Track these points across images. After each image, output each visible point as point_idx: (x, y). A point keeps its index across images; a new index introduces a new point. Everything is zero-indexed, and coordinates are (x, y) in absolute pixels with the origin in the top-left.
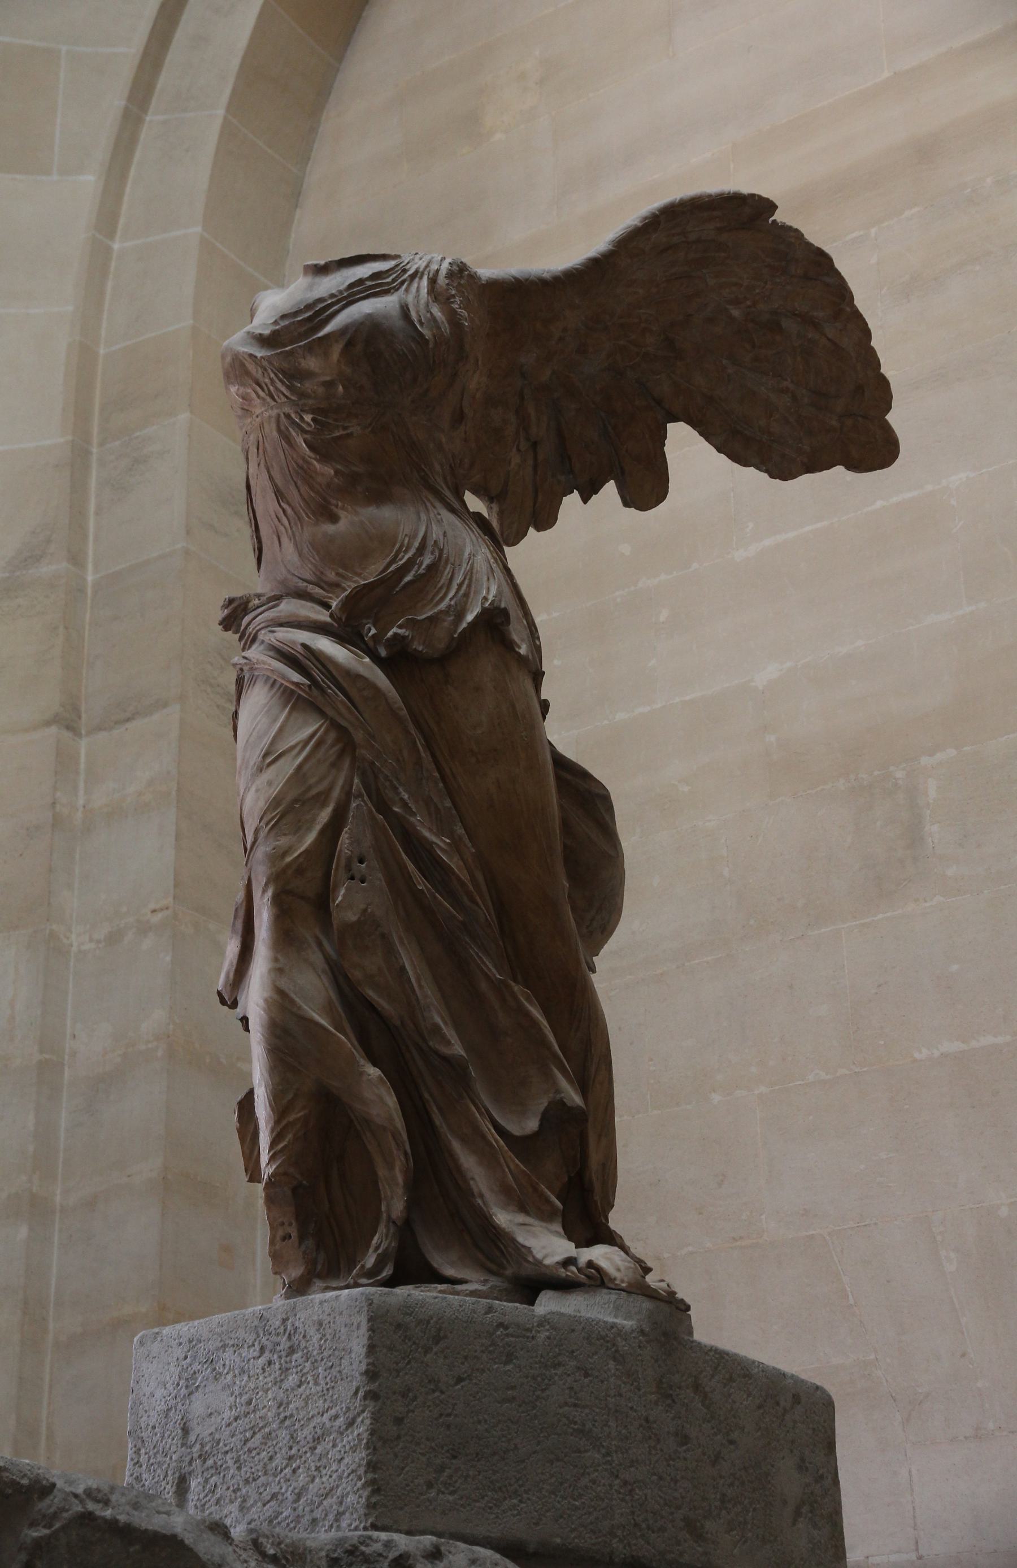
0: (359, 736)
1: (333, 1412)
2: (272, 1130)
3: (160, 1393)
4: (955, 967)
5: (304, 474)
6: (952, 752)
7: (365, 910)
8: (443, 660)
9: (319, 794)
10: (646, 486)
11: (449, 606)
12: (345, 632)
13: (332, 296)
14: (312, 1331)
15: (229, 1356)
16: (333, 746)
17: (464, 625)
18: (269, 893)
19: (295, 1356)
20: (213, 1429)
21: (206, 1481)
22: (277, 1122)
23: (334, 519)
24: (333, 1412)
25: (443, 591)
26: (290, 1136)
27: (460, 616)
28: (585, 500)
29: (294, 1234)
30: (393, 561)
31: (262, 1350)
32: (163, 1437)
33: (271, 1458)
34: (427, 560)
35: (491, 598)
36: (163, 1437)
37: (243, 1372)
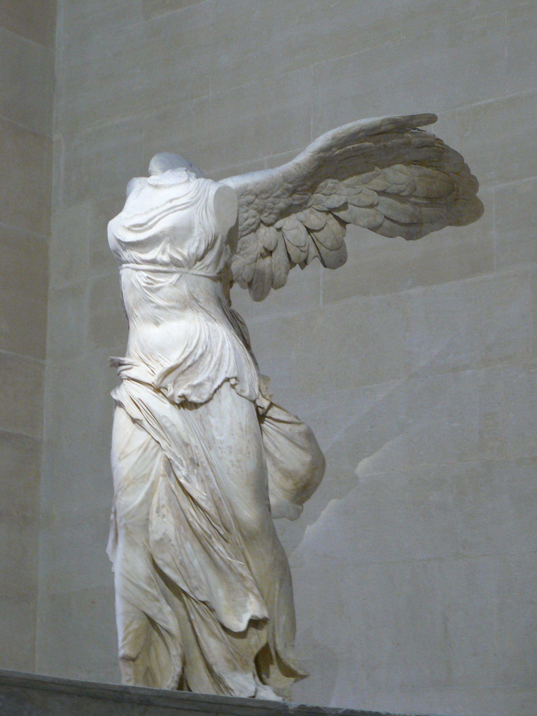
0: (164, 444)
7: (164, 534)
8: (207, 402)
9: (144, 476)
10: (335, 258)
11: (208, 378)
12: (158, 390)
13: (157, 208)
16: (152, 449)
17: (216, 386)
22: (124, 631)
25: (207, 368)
26: (130, 637)
27: (213, 382)
28: (302, 267)
30: (183, 353)
34: (199, 351)
35: (229, 371)
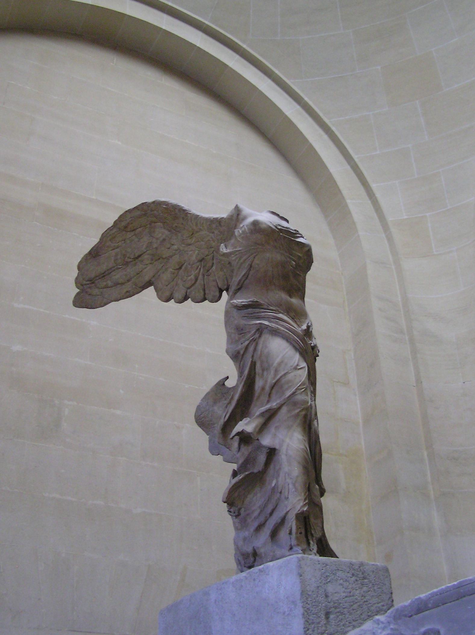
1: (382, 603)
2: (305, 495)
3: (313, 579)
4: (63, 471)
5: (285, 277)
6: (75, 403)
14: (371, 573)
15: (340, 573)
18: (303, 413)
19: (366, 581)
20: (337, 599)
21: (338, 616)
23: (291, 296)
24: (382, 603)
29: (303, 532)
31: (353, 575)
32: (317, 596)
33: (361, 614)
36: (317, 596)
37: (346, 581)
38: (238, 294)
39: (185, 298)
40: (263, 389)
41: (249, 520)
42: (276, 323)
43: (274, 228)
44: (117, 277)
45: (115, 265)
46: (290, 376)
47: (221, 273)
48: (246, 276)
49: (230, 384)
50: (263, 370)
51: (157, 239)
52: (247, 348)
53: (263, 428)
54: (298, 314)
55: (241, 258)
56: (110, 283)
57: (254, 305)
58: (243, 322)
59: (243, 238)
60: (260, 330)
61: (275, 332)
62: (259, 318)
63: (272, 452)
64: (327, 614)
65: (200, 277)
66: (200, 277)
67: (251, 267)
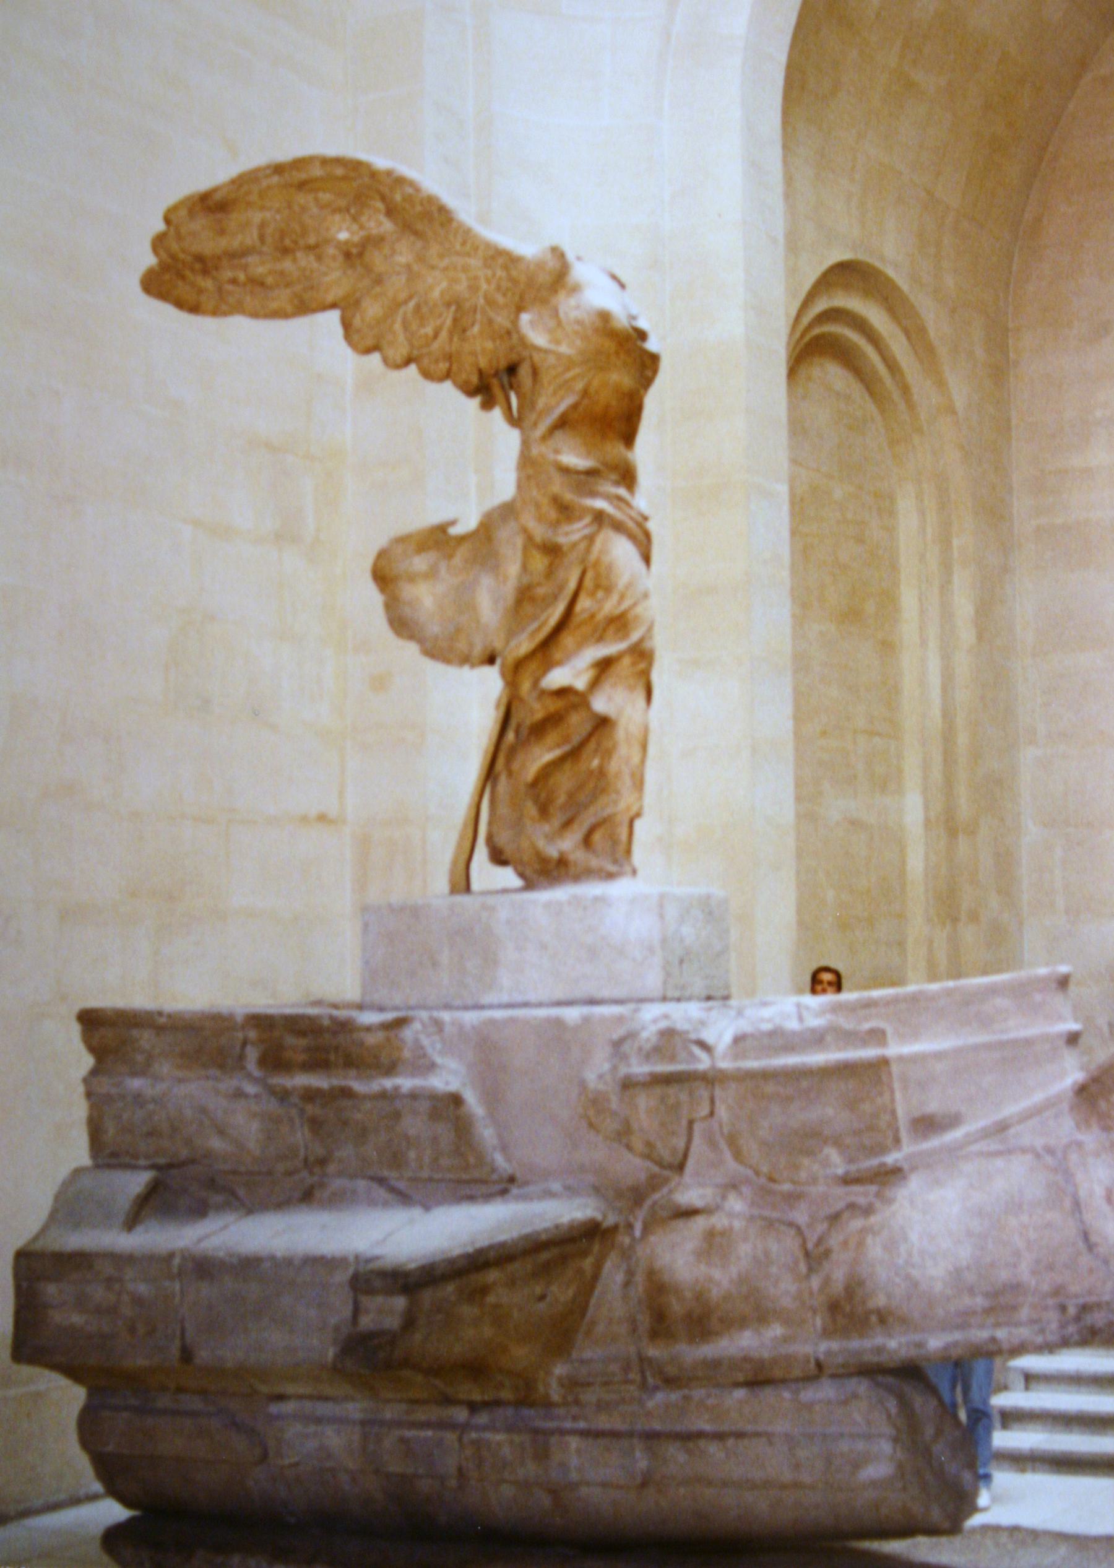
38: (559, 435)
39: (407, 362)
40: (592, 616)
41: (551, 810)
42: (619, 508)
43: (631, 331)
44: (261, 270)
45: (258, 243)
46: (639, 610)
47: (489, 345)
48: (575, 407)
49: (453, 531)
50: (598, 586)
51: (362, 227)
52: (574, 545)
53: (595, 684)
54: (627, 476)
55: (568, 369)
56: (242, 277)
57: (591, 473)
58: (568, 496)
59: (576, 333)
60: (599, 517)
61: (618, 527)
62: (594, 494)
63: (603, 723)
64: (681, 962)
65: (444, 334)
66: (444, 334)
67: (585, 393)
